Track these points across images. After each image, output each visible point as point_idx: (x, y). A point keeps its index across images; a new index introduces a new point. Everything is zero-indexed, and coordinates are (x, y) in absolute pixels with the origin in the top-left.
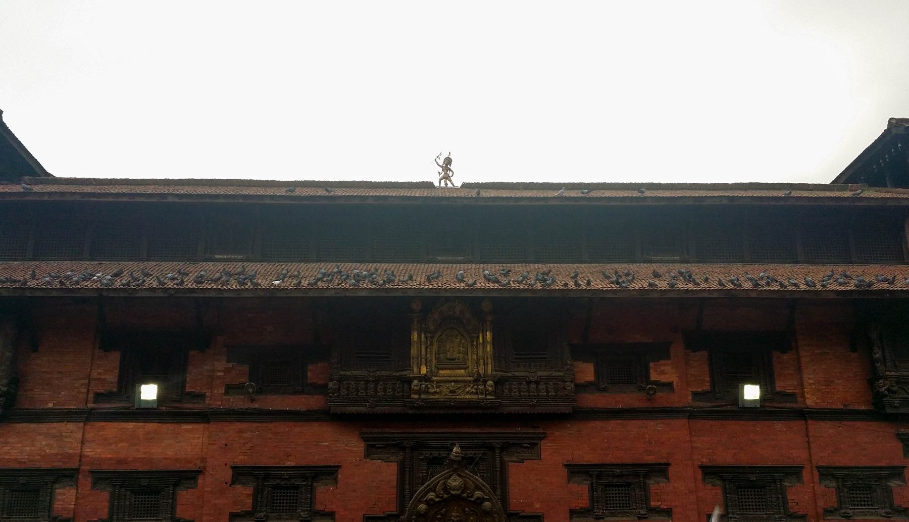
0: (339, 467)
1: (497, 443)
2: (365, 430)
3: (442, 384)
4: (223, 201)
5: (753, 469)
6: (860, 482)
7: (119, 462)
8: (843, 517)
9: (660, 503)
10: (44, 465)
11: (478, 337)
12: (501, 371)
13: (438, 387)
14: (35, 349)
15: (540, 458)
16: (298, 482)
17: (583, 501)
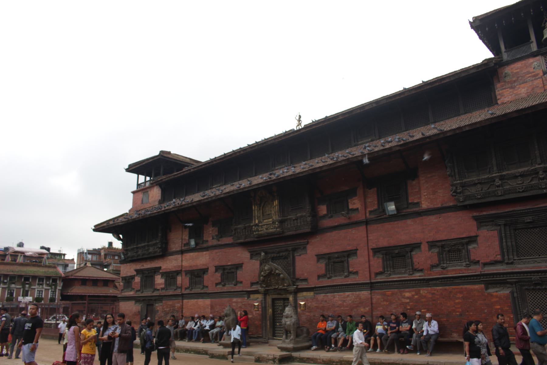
0: (243, 264)
1: (290, 248)
3: (263, 226)
4: (203, 167)
5: (396, 247)
6: (453, 247)
7: (191, 267)
9: (353, 269)
10: (174, 270)
11: (274, 203)
12: (283, 217)
13: (262, 228)
14: (170, 231)
15: (306, 253)
16: (233, 270)
17: (323, 271)
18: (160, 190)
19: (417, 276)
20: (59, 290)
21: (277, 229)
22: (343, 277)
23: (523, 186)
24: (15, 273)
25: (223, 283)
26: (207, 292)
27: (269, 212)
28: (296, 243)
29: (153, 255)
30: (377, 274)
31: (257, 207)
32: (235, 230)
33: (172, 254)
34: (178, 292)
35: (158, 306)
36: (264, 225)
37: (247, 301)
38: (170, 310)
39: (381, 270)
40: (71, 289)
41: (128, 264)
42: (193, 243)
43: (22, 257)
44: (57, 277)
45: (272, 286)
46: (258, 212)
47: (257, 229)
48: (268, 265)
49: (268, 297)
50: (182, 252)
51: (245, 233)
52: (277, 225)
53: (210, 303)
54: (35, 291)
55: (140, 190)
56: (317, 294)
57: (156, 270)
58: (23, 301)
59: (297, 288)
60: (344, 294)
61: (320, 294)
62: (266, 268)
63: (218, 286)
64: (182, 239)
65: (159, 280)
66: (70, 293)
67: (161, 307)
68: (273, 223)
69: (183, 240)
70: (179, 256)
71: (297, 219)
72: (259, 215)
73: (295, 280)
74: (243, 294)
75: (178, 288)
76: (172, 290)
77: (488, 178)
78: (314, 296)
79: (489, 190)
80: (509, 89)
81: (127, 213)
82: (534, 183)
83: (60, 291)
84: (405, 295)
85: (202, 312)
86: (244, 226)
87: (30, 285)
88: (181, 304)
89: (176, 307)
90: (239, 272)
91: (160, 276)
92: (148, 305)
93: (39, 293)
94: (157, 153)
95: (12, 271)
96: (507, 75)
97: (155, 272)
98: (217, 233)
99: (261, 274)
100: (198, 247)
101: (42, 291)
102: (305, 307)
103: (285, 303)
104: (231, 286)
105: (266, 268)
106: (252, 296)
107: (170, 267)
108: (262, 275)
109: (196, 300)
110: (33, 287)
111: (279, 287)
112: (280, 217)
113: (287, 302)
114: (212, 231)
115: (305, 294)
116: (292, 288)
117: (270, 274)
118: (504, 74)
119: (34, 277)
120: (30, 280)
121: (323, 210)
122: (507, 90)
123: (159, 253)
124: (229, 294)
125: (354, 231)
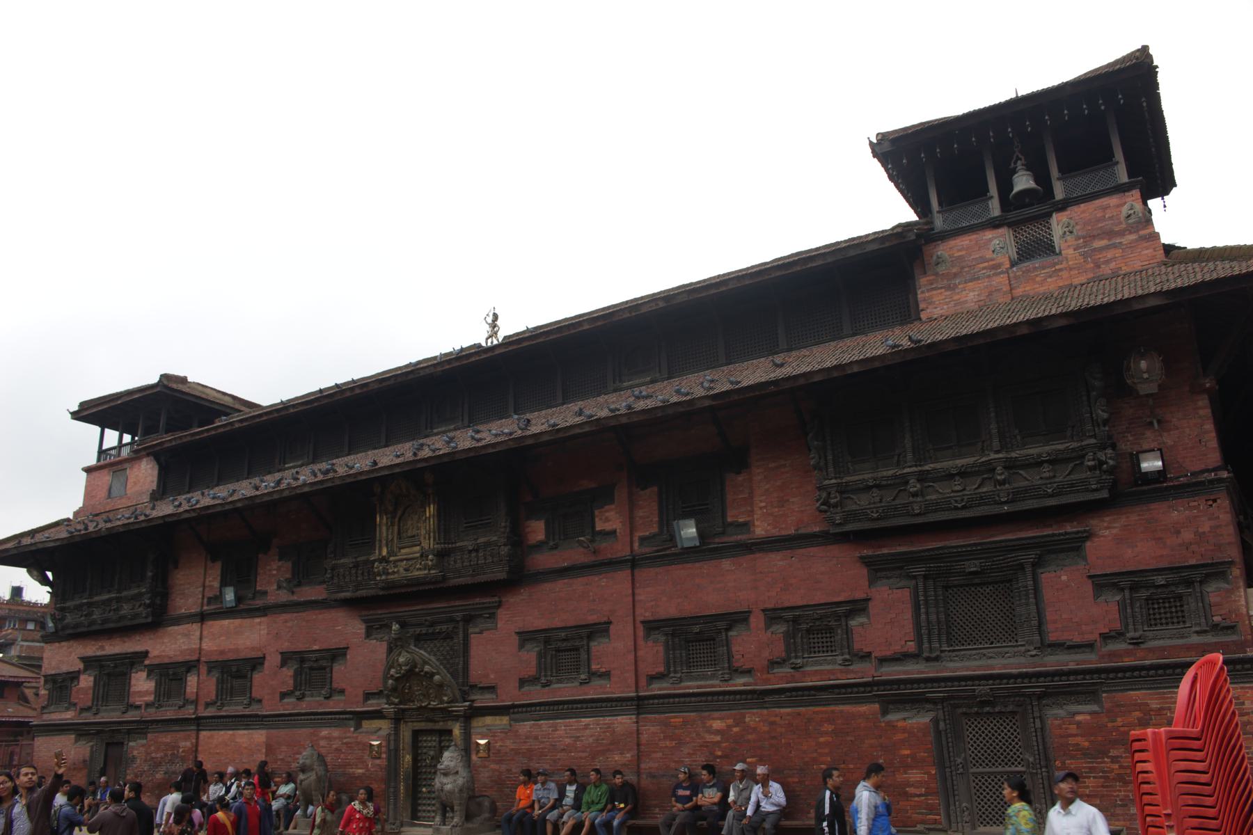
0: (348, 648)
1: (459, 616)
2: (364, 613)
3: (399, 563)
4: (265, 418)
5: (695, 619)
6: (817, 623)
7: (222, 652)
8: (1130, 643)
9: (599, 666)
10: (180, 659)
11: (425, 511)
12: (445, 543)
14: (176, 567)
15: (496, 628)
16: (323, 663)
17: (532, 671)
18: (157, 467)
19: (740, 683)
21: (429, 570)
22: (576, 684)
23: (964, 495)
25: (298, 693)
26: (260, 713)
27: (415, 532)
28: (473, 604)
29: (128, 623)
30: (652, 678)
31: (387, 519)
32: (333, 569)
33: (179, 620)
34: (189, 712)
35: (136, 748)
36: (402, 560)
37: (355, 735)
38: (166, 755)
39: (661, 669)
42: (230, 595)
45: (413, 701)
46: (388, 529)
47: (384, 568)
48: (406, 654)
49: (402, 726)
50: (202, 617)
51: (357, 577)
52: (431, 561)
53: (264, 740)
56: (516, 720)
57: (137, 659)
59: (471, 707)
60: (577, 722)
61: (523, 721)
62: (401, 660)
63: (286, 700)
64: (204, 587)
65: (142, 684)
67: (142, 749)
68: (422, 556)
69: (207, 589)
70: (196, 627)
71: (477, 551)
72: (390, 537)
73: (468, 688)
74: (346, 719)
75: (187, 702)
76: (173, 708)
77: (895, 477)
78: (511, 725)
79: (897, 502)
80: (943, 290)
81: (68, 520)
82: (985, 490)
84: (711, 726)
85: (244, 761)
86: (354, 560)
88: (194, 741)
89: (181, 750)
90: (338, 668)
91: (144, 674)
92: (108, 744)
94: (153, 379)
96: (941, 260)
97: (132, 664)
98: (288, 576)
99: (388, 673)
100: (242, 607)
102: (489, 750)
103: (444, 740)
104: (318, 699)
105: (401, 660)
106: (367, 725)
107: (171, 653)
108: (392, 676)
109: (231, 732)
111: (429, 704)
112: (438, 544)
113: (447, 738)
114: (279, 569)
115: (489, 720)
116: (461, 707)
117: (411, 673)
118: (935, 258)
121: (537, 530)
122: (939, 291)
123: (146, 617)
124: (311, 720)
125: (605, 580)
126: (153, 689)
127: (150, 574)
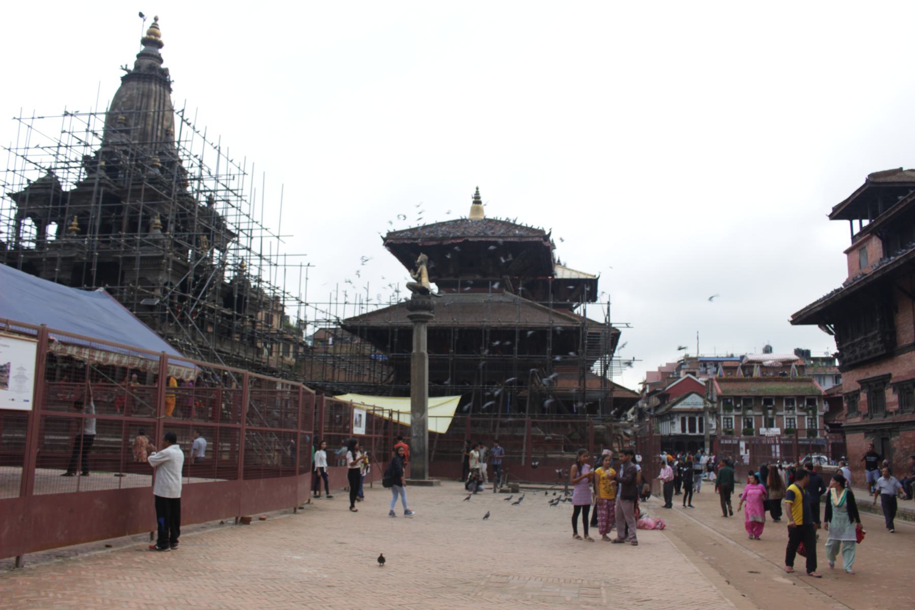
10: (909, 378)
14: (897, 312)
20: (820, 416)
24: (750, 394)
35: (895, 441)
38: (911, 447)
40: (840, 414)
41: (850, 372)
43: (759, 367)
44: (813, 396)
54: (783, 419)
55: (858, 244)
57: (884, 380)
58: (766, 434)
65: (891, 397)
66: (837, 420)
67: (898, 442)
81: (841, 288)
83: (822, 419)
87: (775, 410)
92: (883, 439)
93: (790, 422)
94: (863, 182)
95: (746, 391)
101: (794, 419)
107: (903, 374)
110: (779, 413)
119: (779, 398)
120: (774, 403)
123: (882, 350)
126: (897, 400)
127: (878, 320)
